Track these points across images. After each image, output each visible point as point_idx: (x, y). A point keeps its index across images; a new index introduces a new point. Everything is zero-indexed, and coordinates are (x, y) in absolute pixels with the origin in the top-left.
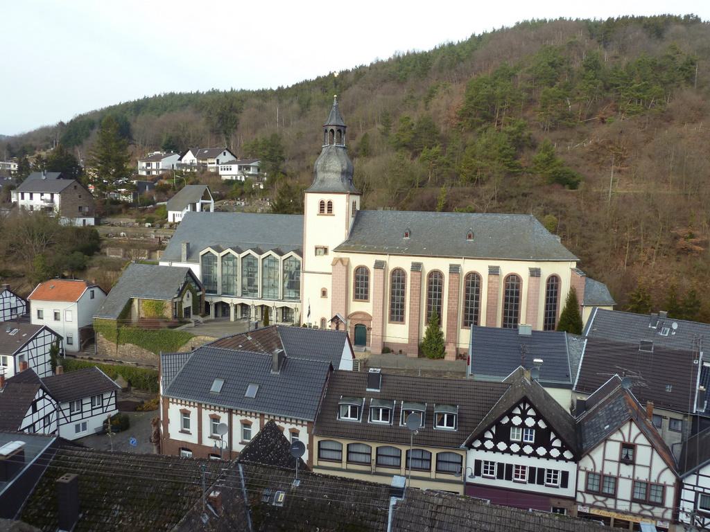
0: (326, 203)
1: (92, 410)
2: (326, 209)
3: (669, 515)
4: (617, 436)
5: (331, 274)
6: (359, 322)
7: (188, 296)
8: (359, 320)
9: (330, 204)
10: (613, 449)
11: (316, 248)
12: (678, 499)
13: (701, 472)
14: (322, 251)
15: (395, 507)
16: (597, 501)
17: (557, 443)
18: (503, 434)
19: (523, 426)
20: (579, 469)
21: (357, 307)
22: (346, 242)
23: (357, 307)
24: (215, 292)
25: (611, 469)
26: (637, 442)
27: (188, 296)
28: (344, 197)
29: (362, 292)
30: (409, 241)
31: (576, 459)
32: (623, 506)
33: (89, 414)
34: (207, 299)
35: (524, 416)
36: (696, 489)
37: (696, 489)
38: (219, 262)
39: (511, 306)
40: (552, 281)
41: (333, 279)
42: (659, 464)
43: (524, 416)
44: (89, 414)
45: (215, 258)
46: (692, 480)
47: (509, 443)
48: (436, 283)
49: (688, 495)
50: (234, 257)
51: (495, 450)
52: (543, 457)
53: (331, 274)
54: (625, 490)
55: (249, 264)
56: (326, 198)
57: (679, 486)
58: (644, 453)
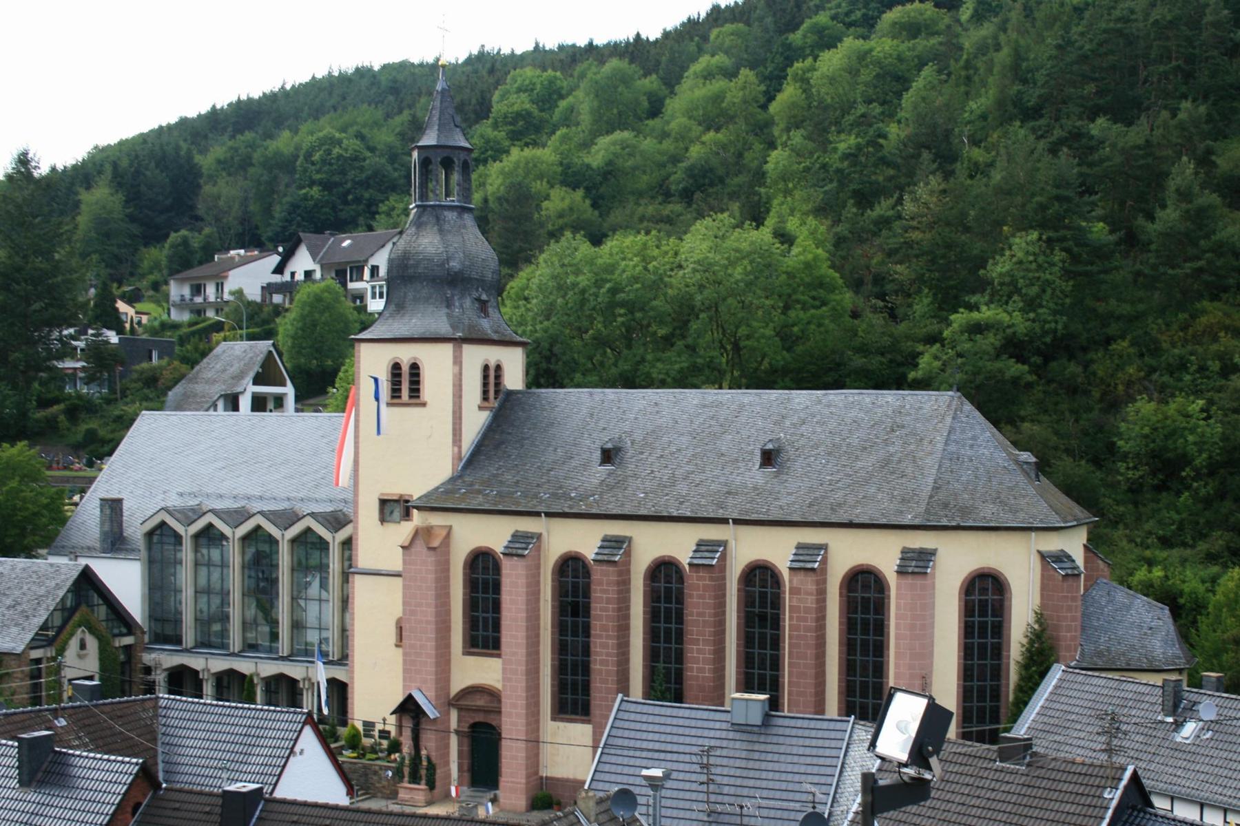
0: (405, 369)
5: (398, 575)
6: (480, 718)
7: (83, 646)
8: (478, 710)
9: (415, 368)
11: (383, 503)
14: (397, 514)
24: (177, 640)
27: (83, 646)
28: (447, 350)
34: (148, 658)
39: (865, 667)
41: (405, 587)
45: (178, 538)
50: (223, 537)
53: (398, 575)
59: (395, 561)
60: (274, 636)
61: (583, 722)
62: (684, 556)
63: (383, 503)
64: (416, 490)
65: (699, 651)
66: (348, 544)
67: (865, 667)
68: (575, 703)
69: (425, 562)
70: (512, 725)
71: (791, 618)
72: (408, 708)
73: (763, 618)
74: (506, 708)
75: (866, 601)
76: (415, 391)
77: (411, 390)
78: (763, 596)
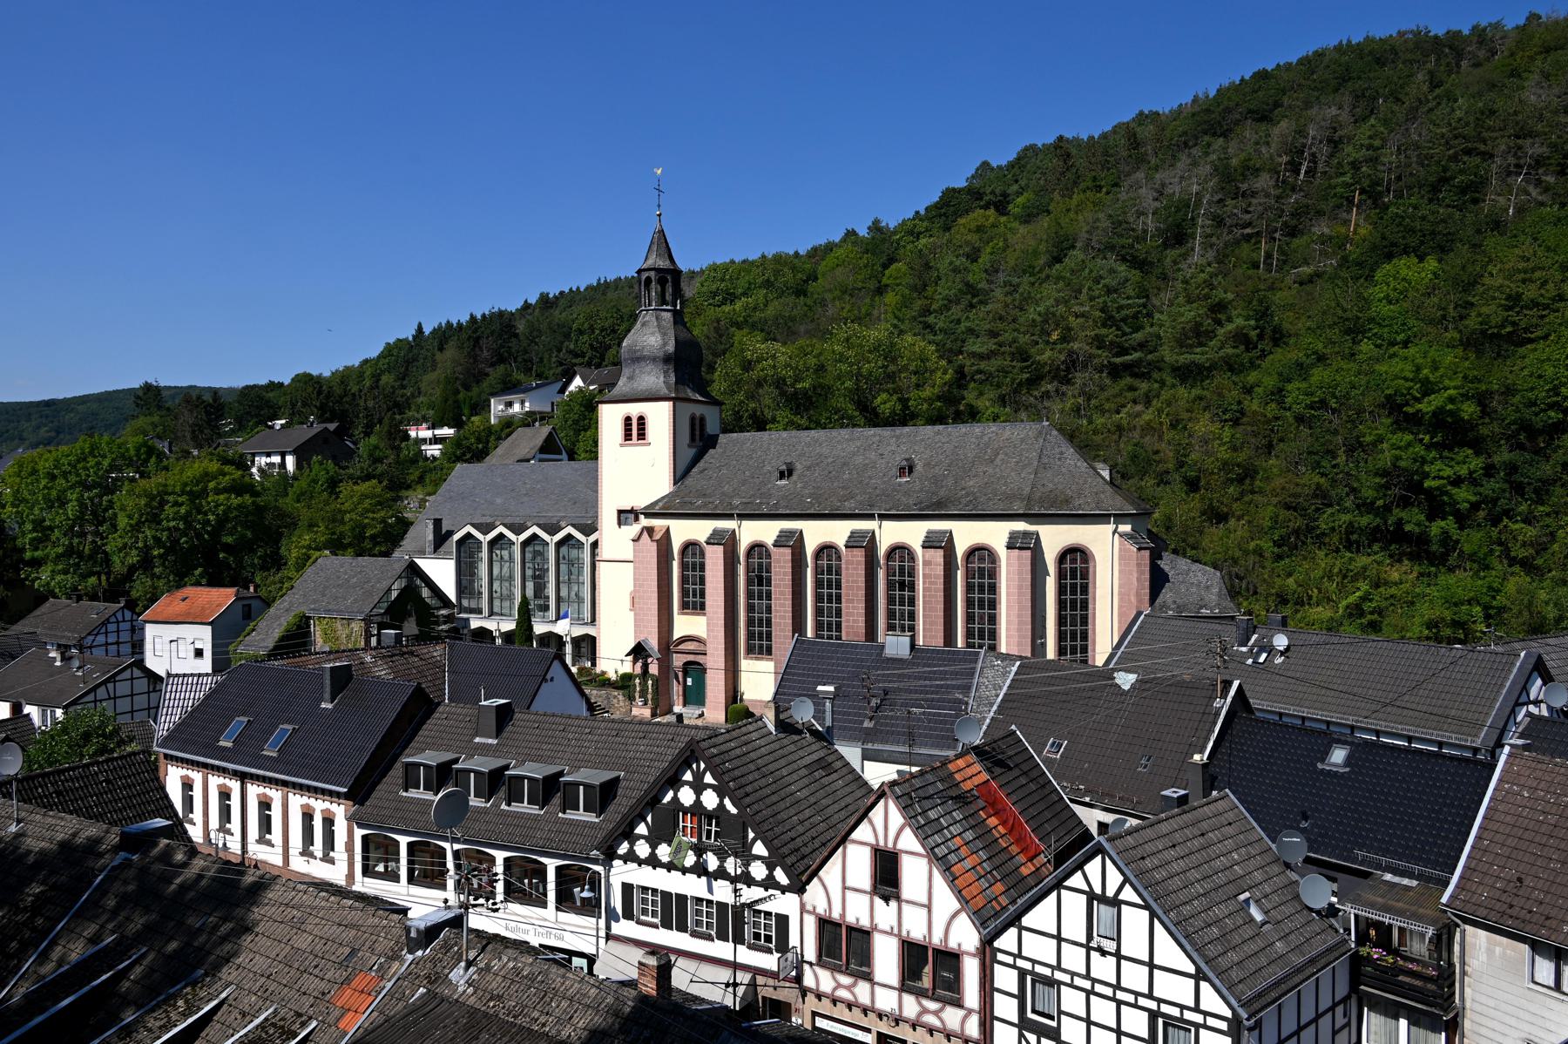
6: (691, 658)
9: (641, 419)
10: (856, 862)
11: (620, 512)
13: (1027, 921)
14: (632, 516)
17: (759, 849)
19: (697, 808)
20: (803, 909)
21: (684, 625)
23: (684, 625)
25: (858, 911)
26: (900, 846)
29: (695, 595)
32: (887, 1000)
36: (1020, 963)
39: (981, 617)
42: (946, 901)
43: (698, 787)
48: (830, 572)
49: (1005, 978)
51: (653, 861)
54: (886, 959)
55: (536, 554)
56: (634, 409)
57: (987, 954)
59: (628, 551)
60: (546, 608)
61: (767, 660)
62: (840, 541)
63: (620, 512)
64: (641, 502)
65: (854, 608)
66: (595, 545)
67: (981, 617)
68: (761, 646)
69: (650, 548)
70: (715, 660)
71: (924, 583)
72: (638, 652)
73: (902, 586)
74: (710, 649)
75: (981, 570)
76: (642, 435)
77: (639, 435)
78: (902, 568)
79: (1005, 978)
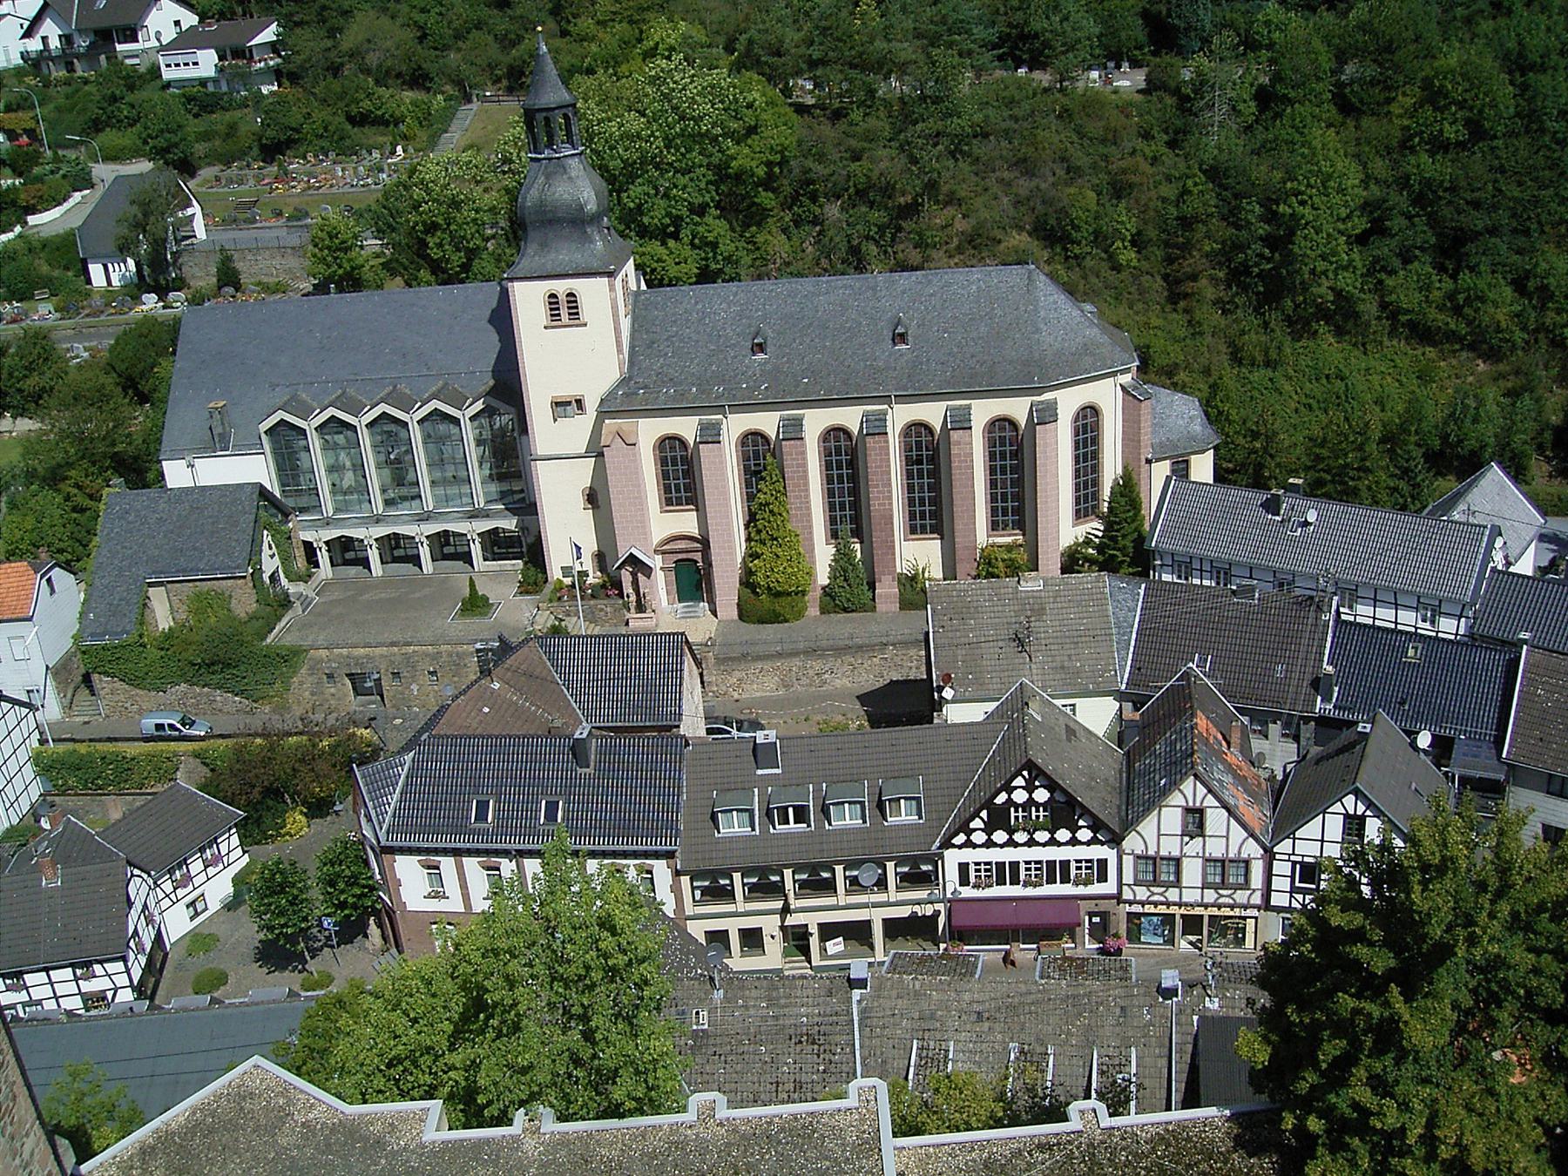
0: (562, 298)
1: (206, 867)
2: (564, 313)
3: (1257, 899)
4: (1176, 799)
10: (1171, 817)
12: (1269, 875)
13: (1298, 835)
15: (859, 1002)
16: (1153, 894)
18: (999, 819)
22: (623, 382)
25: (1170, 847)
26: (1205, 804)
30: (766, 362)
31: (1115, 840)
32: (1190, 896)
33: (203, 877)
35: (1030, 788)
36: (1292, 858)
37: (1292, 858)
38: (315, 441)
40: (1085, 417)
44: (203, 877)
46: (1284, 846)
47: (1011, 832)
49: (1282, 868)
51: (989, 844)
52: (1066, 844)
54: (1192, 872)
56: (561, 287)
57: (1270, 856)
58: (1216, 819)
79: (1282, 868)
